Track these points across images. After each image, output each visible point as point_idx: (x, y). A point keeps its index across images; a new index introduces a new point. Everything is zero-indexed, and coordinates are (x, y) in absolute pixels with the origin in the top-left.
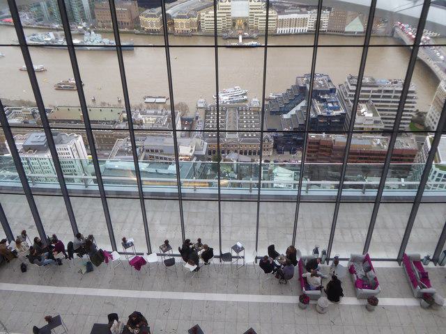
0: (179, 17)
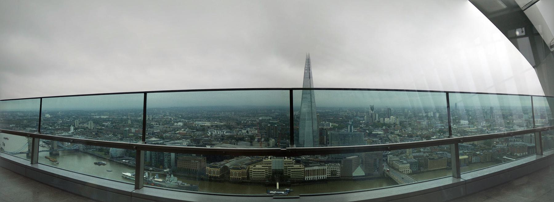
0: (233, 169)
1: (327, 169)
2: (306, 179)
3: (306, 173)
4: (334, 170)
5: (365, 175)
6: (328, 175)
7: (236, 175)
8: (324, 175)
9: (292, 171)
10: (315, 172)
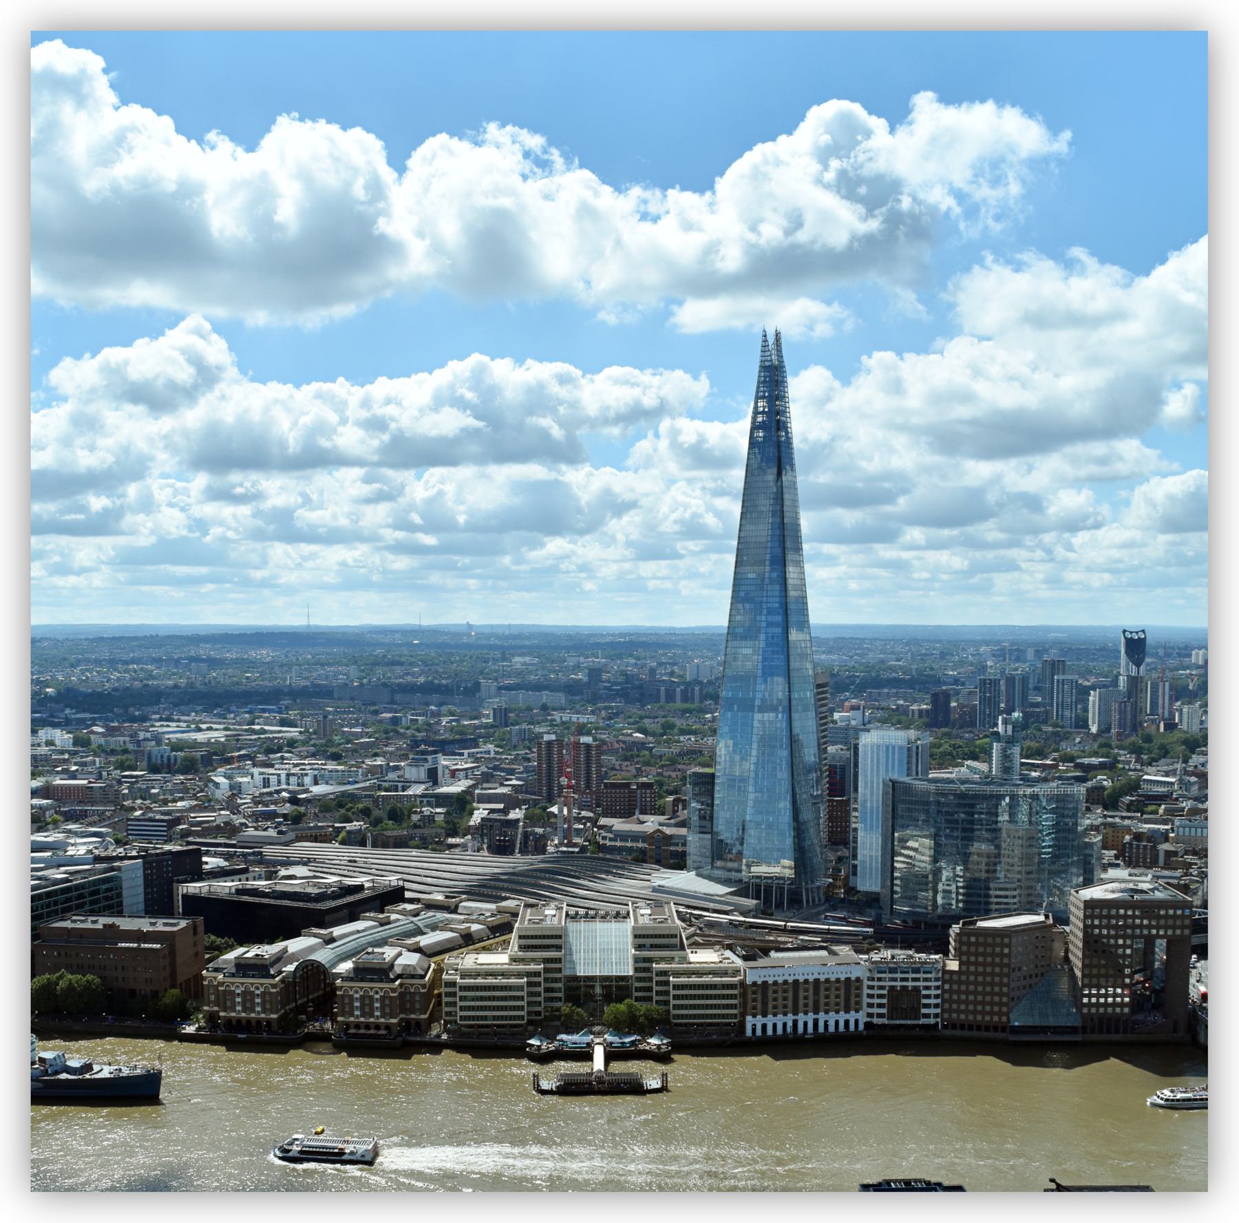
1: (866, 983)
2: (749, 1032)
3: (750, 996)
4: (904, 987)
5: (1084, 1028)
6: (870, 1015)
7: (367, 1008)
8: (852, 1012)
9: (676, 987)
10: (801, 994)
